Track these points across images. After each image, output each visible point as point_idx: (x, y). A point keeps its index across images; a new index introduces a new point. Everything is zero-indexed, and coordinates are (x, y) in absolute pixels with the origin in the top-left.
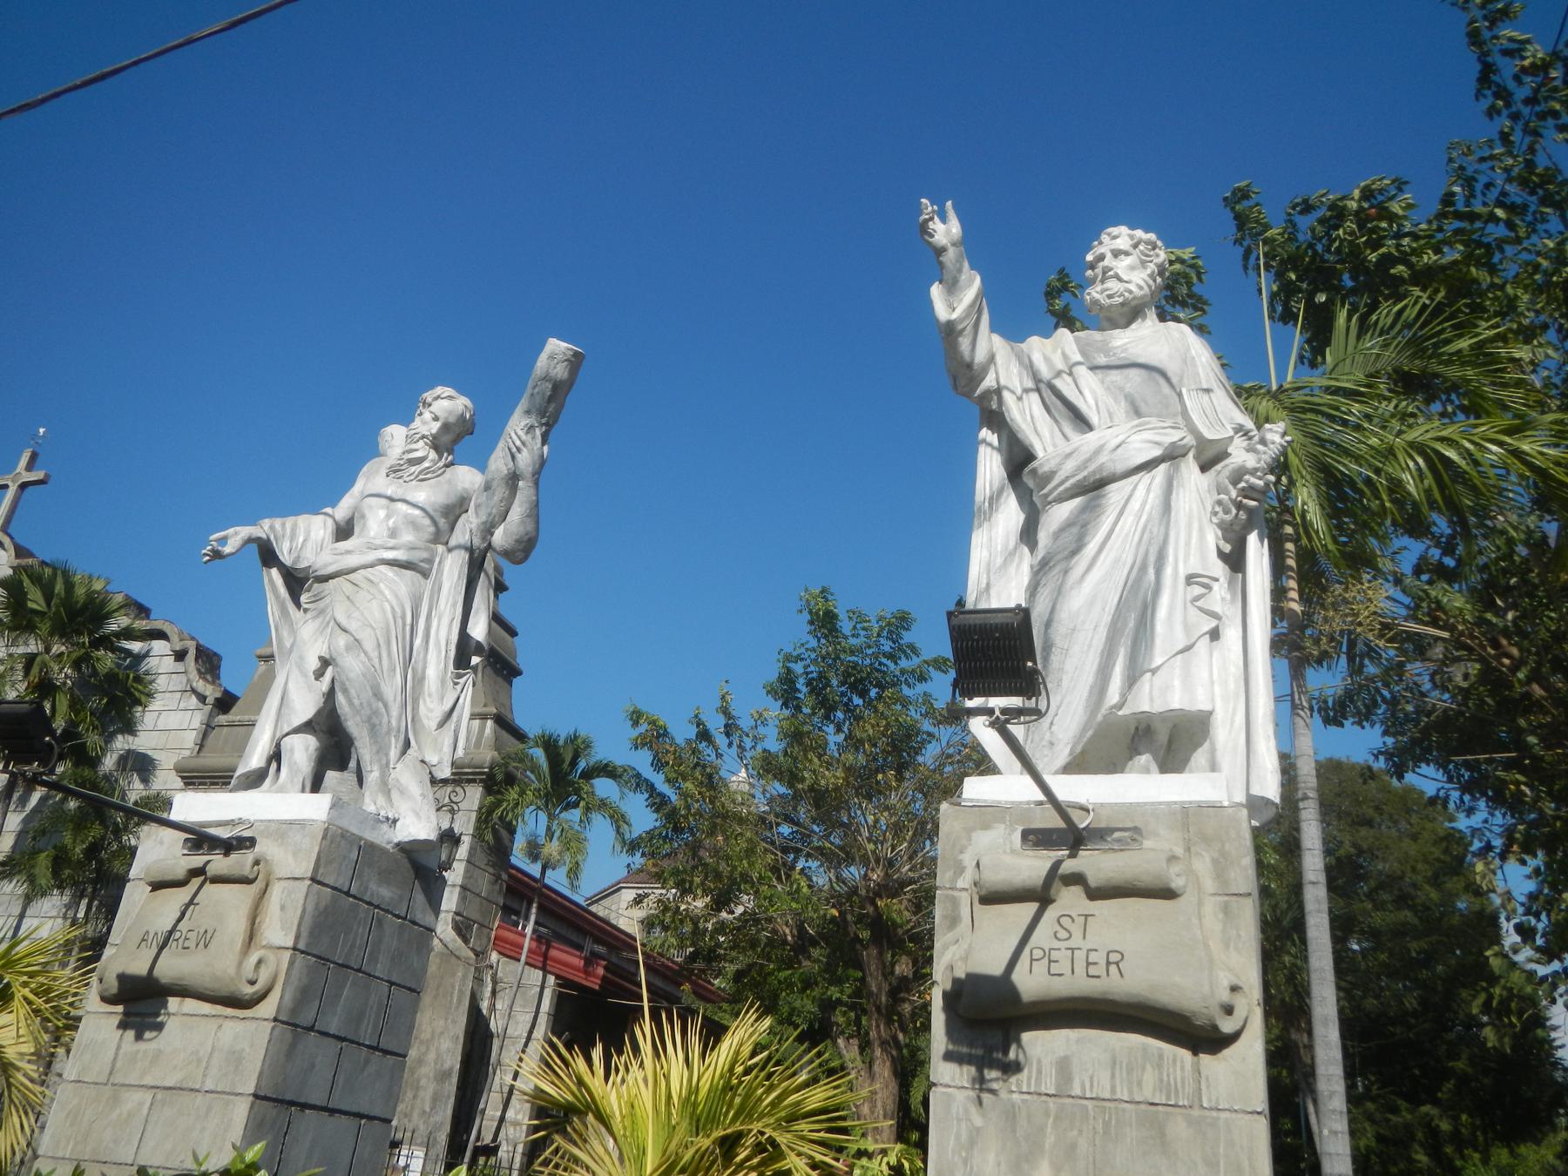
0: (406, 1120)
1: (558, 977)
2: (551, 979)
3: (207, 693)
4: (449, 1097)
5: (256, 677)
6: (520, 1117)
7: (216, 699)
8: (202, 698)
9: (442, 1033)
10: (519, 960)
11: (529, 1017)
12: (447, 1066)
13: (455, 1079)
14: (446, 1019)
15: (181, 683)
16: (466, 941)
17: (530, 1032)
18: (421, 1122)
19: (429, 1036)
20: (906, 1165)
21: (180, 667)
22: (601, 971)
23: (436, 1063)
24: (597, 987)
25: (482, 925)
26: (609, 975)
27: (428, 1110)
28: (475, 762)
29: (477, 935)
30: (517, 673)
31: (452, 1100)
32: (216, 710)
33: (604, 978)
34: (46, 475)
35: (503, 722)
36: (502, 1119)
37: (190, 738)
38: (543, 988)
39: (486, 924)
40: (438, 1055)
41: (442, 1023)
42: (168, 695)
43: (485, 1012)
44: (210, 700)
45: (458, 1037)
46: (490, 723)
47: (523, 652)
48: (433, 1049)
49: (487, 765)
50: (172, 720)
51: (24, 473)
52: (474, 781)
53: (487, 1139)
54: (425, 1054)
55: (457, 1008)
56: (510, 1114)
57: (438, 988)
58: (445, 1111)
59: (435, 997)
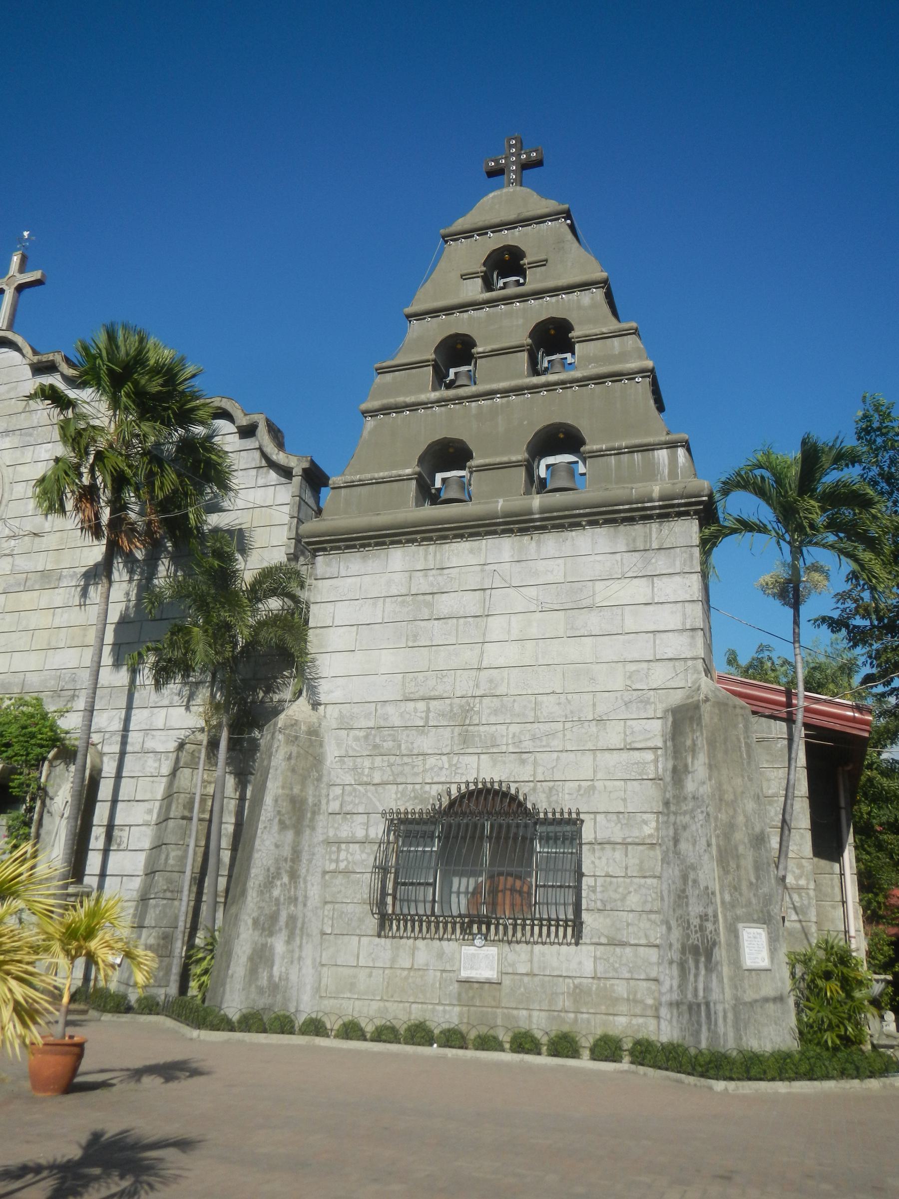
3: (292, 464)
5: (365, 434)
6: (802, 882)
7: (304, 470)
8: (286, 472)
9: (743, 793)
15: (254, 459)
18: (752, 895)
21: (250, 443)
23: (747, 828)
27: (754, 881)
32: (304, 482)
34: (43, 275)
37: (283, 515)
38: (790, 740)
40: (746, 816)
41: (739, 781)
42: (240, 473)
44: (297, 471)
46: (681, 452)
49: (706, 492)
50: (257, 496)
51: (18, 275)
52: (686, 513)
54: (733, 817)
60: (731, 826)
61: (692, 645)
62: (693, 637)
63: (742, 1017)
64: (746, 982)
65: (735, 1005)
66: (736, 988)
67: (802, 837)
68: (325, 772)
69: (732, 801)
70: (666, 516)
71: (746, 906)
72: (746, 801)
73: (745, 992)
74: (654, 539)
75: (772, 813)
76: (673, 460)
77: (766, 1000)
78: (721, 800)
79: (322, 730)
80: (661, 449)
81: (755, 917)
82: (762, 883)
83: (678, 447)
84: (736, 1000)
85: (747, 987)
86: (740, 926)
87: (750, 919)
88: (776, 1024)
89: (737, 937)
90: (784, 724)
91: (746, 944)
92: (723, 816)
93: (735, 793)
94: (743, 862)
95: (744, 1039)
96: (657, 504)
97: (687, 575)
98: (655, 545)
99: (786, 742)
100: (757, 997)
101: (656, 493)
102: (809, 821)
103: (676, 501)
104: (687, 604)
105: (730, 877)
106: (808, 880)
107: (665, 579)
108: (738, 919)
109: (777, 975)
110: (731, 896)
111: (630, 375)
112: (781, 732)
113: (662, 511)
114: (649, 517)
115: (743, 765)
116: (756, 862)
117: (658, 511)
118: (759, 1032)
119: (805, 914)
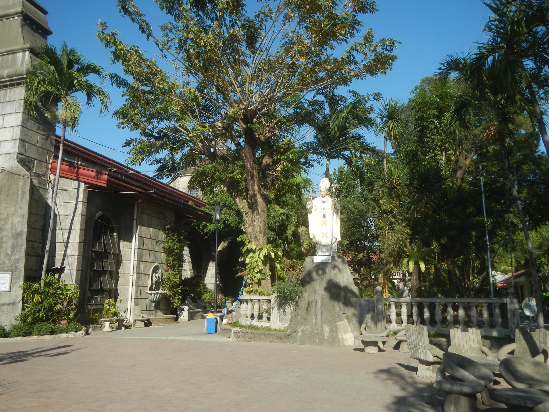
1: (86, 183)
2: (82, 185)
4: (22, 245)
6: (73, 253)
10: (55, 175)
11: (73, 205)
12: (19, 230)
13: (25, 237)
14: (16, 207)
16: (29, 169)
17: (75, 211)
18: (6, 259)
19: (5, 216)
20: (273, 254)
22: (106, 177)
23: (12, 229)
24: (105, 185)
25: (40, 161)
26: (111, 179)
27: (9, 253)
28: (18, 72)
29: (37, 166)
30: (50, 33)
33: (108, 180)
35: (32, 51)
36: (65, 255)
38: (78, 189)
39: (44, 160)
40: (12, 224)
41: (13, 209)
43: (50, 204)
45: (24, 216)
46: (27, 53)
47: (50, 22)
49: (24, 73)
53: (58, 265)
55: (22, 200)
56: (69, 252)
57: (8, 191)
58: (21, 252)
59: (7, 196)
61: (14, 147)
62: (15, 143)
67: (76, 232)
69: (5, 218)
70: (12, 85)
74: (8, 97)
75: (67, 223)
76: (24, 57)
77: (4, 304)
80: (19, 52)
81: (6, 269)
82: (15, 254)
83: (26, 51)
88: (7, 314)
90: (76, 183)
93: (8, 214)
96: (7, 79)
97: (17, 114)
98: (7, 100)
99: (76, 190)
101: (5, 75)
102: (80, 225)
103: (14, 78)
104: (15, 128)
106: (75, 252)
107: (9, 116)
109: (14, 294)
111: (12, 15)
112: (75, 186)
113: (10, 83)
114: (6, 86)
117: (8, 83)
119: (72, 266)
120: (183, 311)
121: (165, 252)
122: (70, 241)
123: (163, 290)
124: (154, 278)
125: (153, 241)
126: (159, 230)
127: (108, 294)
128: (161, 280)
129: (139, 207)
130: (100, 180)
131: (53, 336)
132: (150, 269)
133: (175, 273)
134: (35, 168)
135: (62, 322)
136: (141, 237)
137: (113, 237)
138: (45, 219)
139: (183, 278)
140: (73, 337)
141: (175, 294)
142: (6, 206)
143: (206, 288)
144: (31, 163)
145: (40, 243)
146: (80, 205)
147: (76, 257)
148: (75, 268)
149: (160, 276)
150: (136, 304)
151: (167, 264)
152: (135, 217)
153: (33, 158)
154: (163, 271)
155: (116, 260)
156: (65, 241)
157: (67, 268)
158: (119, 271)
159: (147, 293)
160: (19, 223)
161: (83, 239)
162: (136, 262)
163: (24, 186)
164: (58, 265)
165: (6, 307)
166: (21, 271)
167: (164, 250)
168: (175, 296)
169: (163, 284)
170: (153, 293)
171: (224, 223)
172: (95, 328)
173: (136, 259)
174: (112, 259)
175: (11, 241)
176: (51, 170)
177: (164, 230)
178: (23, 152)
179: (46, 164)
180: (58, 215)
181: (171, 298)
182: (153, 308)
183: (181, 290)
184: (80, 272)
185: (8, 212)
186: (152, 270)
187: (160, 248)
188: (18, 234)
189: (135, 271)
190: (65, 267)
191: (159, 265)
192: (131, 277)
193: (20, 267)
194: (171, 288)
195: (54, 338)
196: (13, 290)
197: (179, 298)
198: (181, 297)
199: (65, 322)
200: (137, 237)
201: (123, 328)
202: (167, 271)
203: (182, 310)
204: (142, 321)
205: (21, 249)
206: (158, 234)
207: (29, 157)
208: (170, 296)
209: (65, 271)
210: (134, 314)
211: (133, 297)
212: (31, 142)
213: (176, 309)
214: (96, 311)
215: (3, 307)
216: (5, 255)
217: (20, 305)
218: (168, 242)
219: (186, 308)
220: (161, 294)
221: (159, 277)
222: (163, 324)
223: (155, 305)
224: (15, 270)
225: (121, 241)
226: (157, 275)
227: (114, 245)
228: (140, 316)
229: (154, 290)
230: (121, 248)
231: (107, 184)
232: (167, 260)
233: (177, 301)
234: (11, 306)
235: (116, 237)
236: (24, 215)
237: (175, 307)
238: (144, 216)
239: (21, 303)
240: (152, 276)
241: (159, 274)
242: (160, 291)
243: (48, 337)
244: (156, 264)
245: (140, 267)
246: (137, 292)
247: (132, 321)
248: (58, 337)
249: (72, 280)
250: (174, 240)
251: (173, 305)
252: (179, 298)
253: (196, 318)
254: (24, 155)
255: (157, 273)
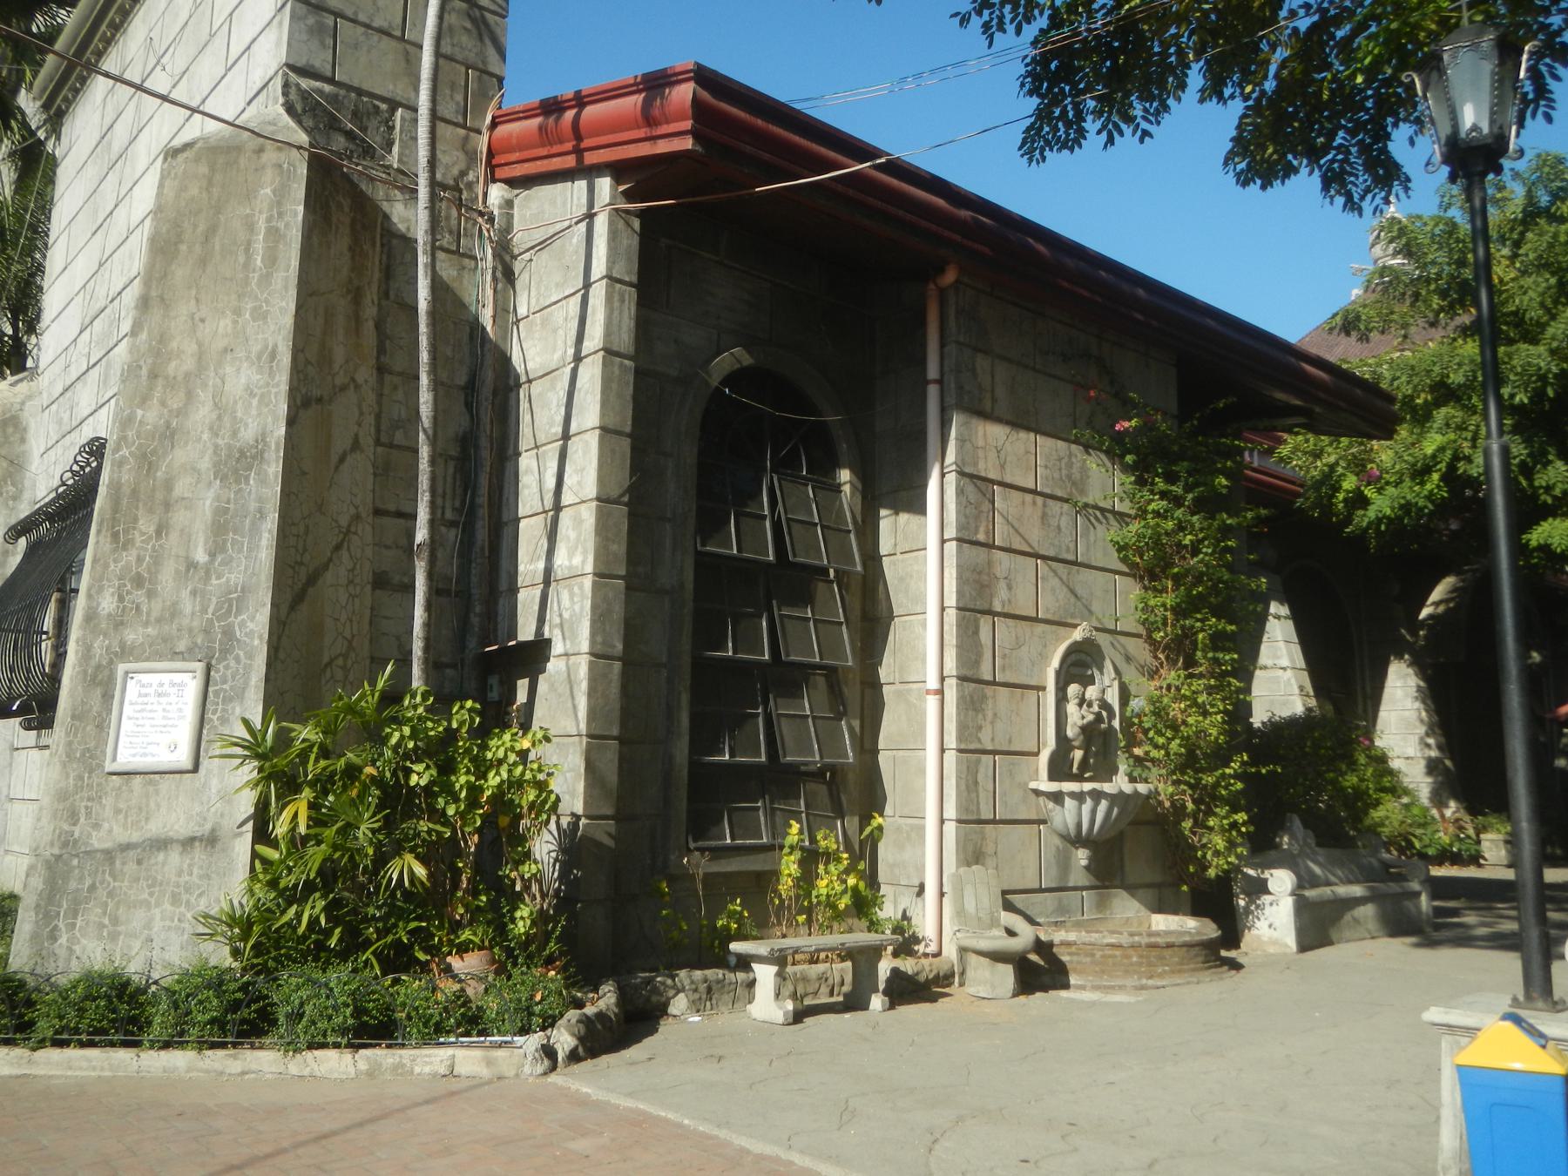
0: (139, 596)
2: (604, 184)
4: (261, 514)
6: (577, 561)
12: (248, 434)
14: (238, 312)
18: (185, 594)
19: (189, 364)
23: (215, 434)
24: (688, 143)
27: (201, 556)
31: (271, 524)
41: (225, 324)
45: (273, 355)
48: (204, 396)
53: (526, 632)
54: (181, 413)
55: (266, 279)
56: (561, 559)
57: (212, 230)
59: (203, 262)
60: (169, 435)
63: (73, 885)
64: (108, 801)
65: (58, 858)
66: (73, 817)
68: (27, 483)
69: (187, 375)
71: (159, 621)
72: (229, 370)
73: (97, 826)
77: (162, 844)
78: (153, 376)
79: (26, 414)
81: (182, 646)
84: (65, 844)
85: (108, 812)
86: (121, 668)
87: (164, 652)
88: (175, 900)
89: (108, 697)
91: (128, 710)
92: (151, 416)
93: (200, 356)
94: (179, 517)
95: (63, 940)
100: (136, 837)
102: (598, 407)
105: (130, 557)
106: (585, 552)
108: (126, 653)
110: (121, 599)
115: (246, 281)
116: (220, 511)
118: (115, 921)
119: (574, 636)
120: (1266, 899)
121: (1135, 572)
122: (567, 498)
123: (1132, 780)
124: (1072, 708)
125: (1055, 507)
126: (1087, 447)
127: (822, 790)
128: (1116, 723)
129: (952, 312)
130: (668, 122)
131: (379, 1056)
132: (1044, 658)
133: (1198, 684)
134: (396, 149)
135: (455, 962)
136: (972, 476)
137: (837, 489)
138: (468, 405)
139: (1258, 718)
140: (485, 1072)
141: (1207, 799)
142: (192, 317)
143: (1391, 773)
144: (373, 123)
145: (453, 524)
146: (598, 293)
147: (588, 582)
148: (585, 646)
149: (1113, 698)
150: (973, 855)
151: (1150, 628)
152: (933, 372)
153: (383, 99)
154: (1131, 675)
155: (856, 613)
156: (549, 503)
157: (558, 648)
158: (884, 673)
159: (1037, 793)
160: (252, 395)
161: (622, 479)
162: (951, 615)
163: (279, 203)
164: (526, 632)
165: (174, 857)
166: (250, 656)
167: (1124, 560)
168: (1210, 813)
169: (1132, 742)
170: (1073, 795)
171: (1450, 477)
172: (707, 997)
173: (951, 600)
174: (834, 603)
175: (211, 494)
176: (489, 162)
177: (1116, 448)
178: (321, 61)
179: (462, 132)
180: (523, 379)
181: (1187, 824)
182: (1078, 877)
183: (1236, 776)
184: (617, 665)
185: (200, 344)
186: (1055, 663)
187: (1100, 543)
188: (242, 453)
189: (951, 666)
190: (549, 641)
191: (1103, 640)
192: (932, 703)
193: (250, 634)
194: (1182, 769)
195: (370, 1074)
196: (205, 763)
197: (1234, 825)
198: (1241, 817)
199: (467, 964)
200: (951, 478)
201: (877, 1002)
202: (1153, 674)
203: (1261, 888)
204: (997, 957)
205: (255, 530)
206: (1084, 470)
207: (360, 92)
208: (1179, 811)
209: (549, 666)
210: (960, 913)
211: (951, 812)
212: (362, 17)
213: (1225, 881)
214: (718, 888)
215: (161, 856)
216: (183, 568)
217: (243, 845)
218: (1142, 513)
219: (1281, 881)
220: (1118, 799)
221: (1105, 705)
222: (1131, 982)
223: (1090, 859)
224: (225, 652)
225: (883, 512)
226: (1092, 692)
227: (834, 530)
228: (994, 923)
229: (1079, 778)
230: (884, 548)
231: (694, 133)
232: (1147, 608)
233: (1219, 842)
234: (198, 853)
235: (847, 489)
236: (276, 345)
237: (1212, 873)
238: (982, 363)
239: (249, 836)
240: (1061, 699)
241: (1105, 687)
242: (1121, 783)
243: (335, 1064)
244: (1078, 635)
245: (978, 645)
246: (969, 784)
247: (950, 952)
248: (395, 1068)
249: (575, 707)
250: (1177, 501)
251: (1204, 866)
252: (1234, 825)
253: (1347, 934)
254: (331, 80)
255: (1088, 681)
